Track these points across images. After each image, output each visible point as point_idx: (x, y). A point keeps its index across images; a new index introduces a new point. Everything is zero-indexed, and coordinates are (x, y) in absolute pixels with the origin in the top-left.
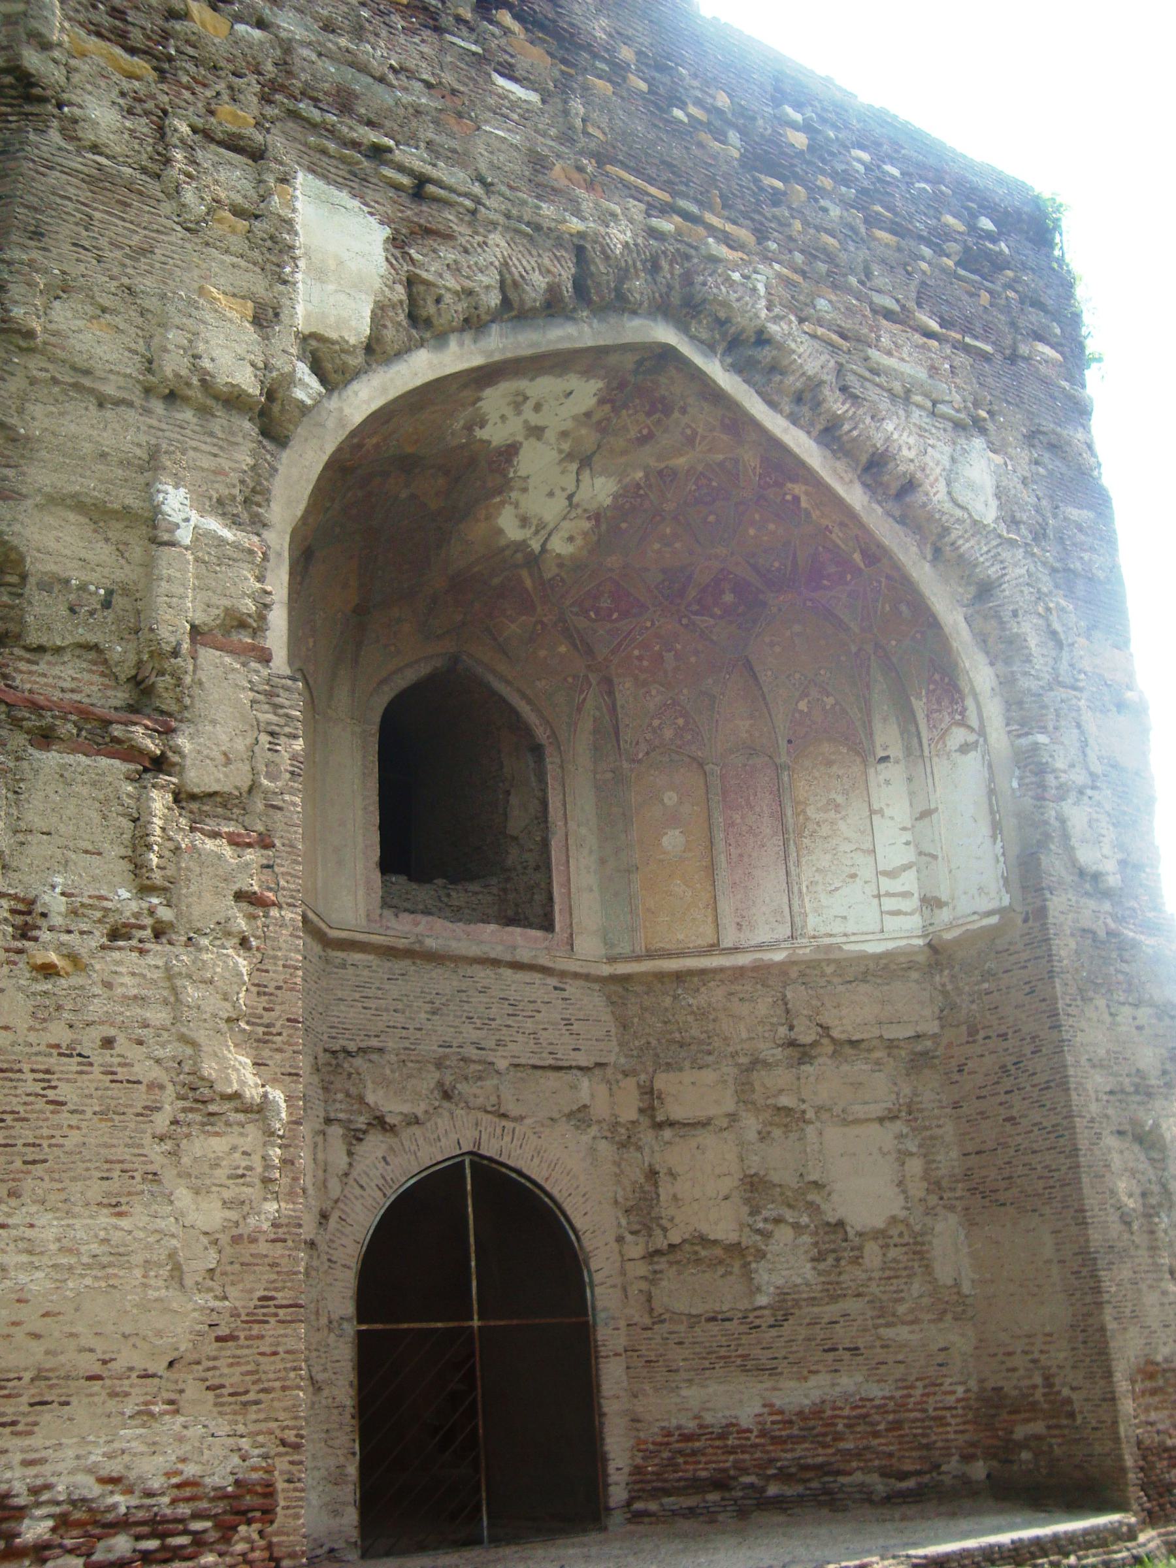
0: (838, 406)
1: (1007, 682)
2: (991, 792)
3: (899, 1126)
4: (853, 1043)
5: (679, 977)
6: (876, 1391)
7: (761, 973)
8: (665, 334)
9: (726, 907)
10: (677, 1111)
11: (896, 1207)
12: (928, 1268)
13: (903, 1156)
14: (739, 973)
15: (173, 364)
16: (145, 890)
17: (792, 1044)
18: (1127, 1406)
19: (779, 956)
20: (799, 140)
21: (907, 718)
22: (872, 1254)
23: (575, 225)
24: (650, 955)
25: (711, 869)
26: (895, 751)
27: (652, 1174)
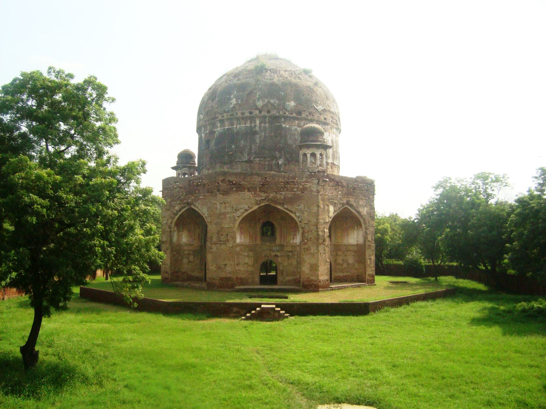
0: (356, 208)
1: (365, 226)
2: (363, 235)
6: (351, 274)
7: (344, 245)
8: (346, 206)
9: (343, 240)
11: (353, 262)
15: (325, 222)
16: (324, 251)
20: (356, 186)
22: (351, 265)
24: (337, 243)
25: (342, 237)
27: (336, 259)
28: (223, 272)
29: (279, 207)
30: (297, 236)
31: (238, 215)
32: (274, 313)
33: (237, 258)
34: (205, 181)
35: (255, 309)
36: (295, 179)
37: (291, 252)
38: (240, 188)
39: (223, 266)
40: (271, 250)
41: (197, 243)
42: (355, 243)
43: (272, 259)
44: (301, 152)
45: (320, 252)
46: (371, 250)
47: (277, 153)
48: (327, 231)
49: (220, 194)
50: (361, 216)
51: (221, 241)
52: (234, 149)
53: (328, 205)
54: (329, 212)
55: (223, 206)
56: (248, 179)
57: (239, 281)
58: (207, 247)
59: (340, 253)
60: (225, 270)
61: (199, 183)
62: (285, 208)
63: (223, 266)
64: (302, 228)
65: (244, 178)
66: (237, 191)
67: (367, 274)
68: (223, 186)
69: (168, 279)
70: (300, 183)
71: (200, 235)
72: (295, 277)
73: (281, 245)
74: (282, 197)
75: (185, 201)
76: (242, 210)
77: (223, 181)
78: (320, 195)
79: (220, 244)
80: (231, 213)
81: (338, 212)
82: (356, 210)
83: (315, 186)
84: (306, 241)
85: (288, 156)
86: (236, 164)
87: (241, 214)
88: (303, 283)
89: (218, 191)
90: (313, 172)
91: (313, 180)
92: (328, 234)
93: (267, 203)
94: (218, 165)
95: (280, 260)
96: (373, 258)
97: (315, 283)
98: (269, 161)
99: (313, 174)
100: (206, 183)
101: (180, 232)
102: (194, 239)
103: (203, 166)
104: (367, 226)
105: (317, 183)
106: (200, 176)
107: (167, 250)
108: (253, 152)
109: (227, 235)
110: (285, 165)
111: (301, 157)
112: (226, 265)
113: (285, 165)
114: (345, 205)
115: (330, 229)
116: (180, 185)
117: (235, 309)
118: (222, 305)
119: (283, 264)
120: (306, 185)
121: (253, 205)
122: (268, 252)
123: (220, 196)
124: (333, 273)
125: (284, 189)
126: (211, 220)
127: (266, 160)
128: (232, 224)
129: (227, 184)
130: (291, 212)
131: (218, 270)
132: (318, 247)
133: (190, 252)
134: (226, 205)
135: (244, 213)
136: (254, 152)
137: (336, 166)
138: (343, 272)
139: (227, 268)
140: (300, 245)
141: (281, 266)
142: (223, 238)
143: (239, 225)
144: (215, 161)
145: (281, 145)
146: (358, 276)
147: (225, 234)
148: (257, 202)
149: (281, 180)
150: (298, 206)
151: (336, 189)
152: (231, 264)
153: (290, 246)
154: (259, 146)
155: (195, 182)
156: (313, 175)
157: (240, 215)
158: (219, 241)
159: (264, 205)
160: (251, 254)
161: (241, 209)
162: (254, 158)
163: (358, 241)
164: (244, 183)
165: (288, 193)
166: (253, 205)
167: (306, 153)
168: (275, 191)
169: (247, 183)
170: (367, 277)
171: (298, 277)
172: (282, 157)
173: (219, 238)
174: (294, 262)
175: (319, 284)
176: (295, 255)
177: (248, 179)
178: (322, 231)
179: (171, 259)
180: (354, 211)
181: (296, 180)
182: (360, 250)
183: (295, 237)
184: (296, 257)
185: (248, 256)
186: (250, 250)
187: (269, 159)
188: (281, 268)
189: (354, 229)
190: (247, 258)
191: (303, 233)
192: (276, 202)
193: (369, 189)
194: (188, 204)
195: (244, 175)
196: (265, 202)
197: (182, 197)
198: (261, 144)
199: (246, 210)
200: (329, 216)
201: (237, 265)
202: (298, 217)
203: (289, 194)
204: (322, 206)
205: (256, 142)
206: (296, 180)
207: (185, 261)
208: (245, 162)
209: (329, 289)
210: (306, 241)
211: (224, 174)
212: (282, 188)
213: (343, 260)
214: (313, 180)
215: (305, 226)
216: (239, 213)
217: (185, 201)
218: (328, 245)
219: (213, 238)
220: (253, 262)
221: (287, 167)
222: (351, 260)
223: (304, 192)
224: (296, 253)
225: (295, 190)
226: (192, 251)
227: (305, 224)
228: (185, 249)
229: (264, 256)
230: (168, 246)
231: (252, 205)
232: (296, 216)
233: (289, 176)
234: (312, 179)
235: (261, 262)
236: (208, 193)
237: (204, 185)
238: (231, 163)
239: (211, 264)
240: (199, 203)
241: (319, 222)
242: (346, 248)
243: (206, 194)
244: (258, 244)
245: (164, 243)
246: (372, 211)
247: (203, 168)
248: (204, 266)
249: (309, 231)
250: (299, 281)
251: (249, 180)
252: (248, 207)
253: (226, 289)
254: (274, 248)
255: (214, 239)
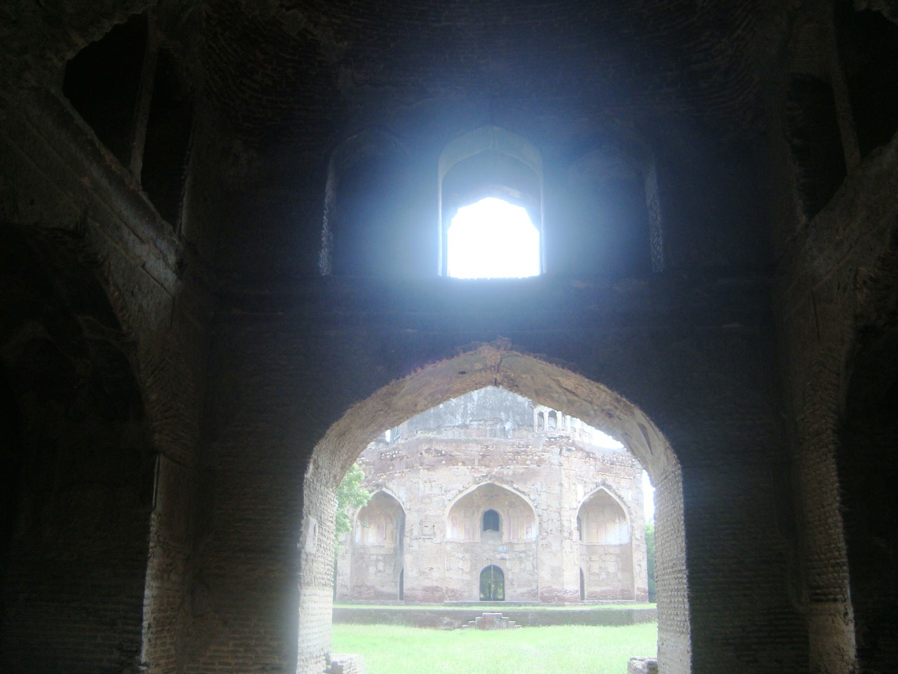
0: (616, 491)
1: (631, 518)
2: (628, 530)
3: (615, 562)
4: (611, 554)
5: (594, 545)
6: (611, 589)
8: (602, 487)
10: (593, 560)
12: (617, 577)
13: (615, 565)
14: (599, 545)
15: (572, 507)
17: (605, 553)
18: (635, 591)
19: (604, 544)
20: (615, 459)
21: (620, 519)
22: (612, 575)
23: (596, 481)
26: (618, 522)
27: (590, 566)
28: (427, 578)
29: (506, 487)
30: (532, 529)
31: (449, 499)
32: (500, 622)
33: (447, 560)
34: (403, 453)
35: (474, 620)
36: (528, 448)
37: (524, 552)
38: (451, 460)
39: (427, 571)
40: (495, 551)
41: (389, 545)
42: (617, 543)
43: (498, 565)
44: (535, 410)
45: (565, 550)
46: (641, 553)
47: (502, 413)
48: (574, 520)
49: (424, 469)
50: (625, 503)
51: (425, 535)
52: (443, 410)
53: (575, 484)
54: (577, 493)
55: (428, 485)
56: (463, 448)
57: (450, 594)
58: (405, 545)
59: (594, 558)
60: (430, 576)
61: (394, 456)
62: (514, 488)
63: (427, 571)
64: (539, 516)
65: (458, 447)
66: (447, 465)
67: (635, 587)
68: (429, 458)
69: (347, 595)
70: (534, 453)
71: (394, 533)
72: (530, 589)
73: (510, 543)
74: (511, 473)
75: (373, 482)
76: (454, 492)
77: (428, 451)
78: (564, 469)
79: (424, 539)
80: (439, 495)
81: (589, 494)
82: (616, 494)
83: (556, 457)
84: (544, 534)
85: (518, 418)
86: (446, 430)
87: (453, 497)
88: (541, 593)
89: (422, 464)
90: (553, 438)
91: (553, 448)
92: (576, 525)
93: (489, 482)
94: (419, 432)
95: (508, 564)
96: (644, 564)
97: (559, 594)
98: (491, 425)
99: (553, 440)
100: (404, 454)
101: (365, 528)
102: (385, 539)
103: (398, 436)
104: (632, 518)
105: (559, 452)
106: (395, 446)
107: (346, 553)
108: (469, 412)
109: (434, 526)
110: (514, 430)
111: (536, 417)
112: (432, 569)
113: (514, 430)
114: (599, 486)
115: (579, 519)
116: (367, 460)
117: (447, 619)
118: (428, 614)
119: (513, 571)
120: (543, 455)
121: (470, 485)
122: (491, 554)
123: (423, 473)
124: (585, 586)
125: (512, 462)
126: (410, 506)
127: (487, 423)
128: (440, 511)
129: (433, 455)
130: (523, 493)
131: (421, 575)
132: (562, 543)
133: (380, 558)
134: (431, 484)
135: (457, 495)
136: (471, 412)
137: (587, 434)
138: (601, 586)
139: (433, 573)
140: (536, 542)
141: (510, 573)
142: (427, 531)
143: (449, 515)
144: (416, 428)
145: (508, 403)
146: (622, 591)
147: (430, 525)
148: (476, 480)
149: (509, 449)
150: (532, 485)
151: (586, 462)
152: (439, 568)
153: (522, 544)
154: (477, 405)
155: (388, 455)
156: (553, 442)
157: (451, 498)
158: (423, 535)
159: (485, 485)
160: (467, 556)
161: (453, 489)
162: (471, 421)
163: (620, 540)
164: (458, 453)
165: (518, 466)
166: (470, 485)
167: (543, 411)
168: (500, 464)
169: (460, 454)
170: (636, 592)
171: (534, 587)
172: (510, 420)
173: (422, 530)
174: (529, 567)
175: (565, 596)
176: (529, 556)
177: (463, 448)
178: (567, 520)
179: (351, 567)
180: (613, 495)
181: (528, 449)
182: (625, 554)
183: (529, 529)
184: (531, 558)
185: (463, 559)
186: (466, 551)
187: (492, 422)
188: (510, 577)
189: (614, 522)
190: (462, 561)
191: (540, 523)
192: (503, 481)
193: (634, 465)
194: (378, 486)
195: (457, 442)
196: (487, 479)
197: (370, 477)
198: (480, 402)
199: (460, 492)
200: (576, 501)
201: (447, 570)
202: (534, 500)
203: (519, 468)
204: (566, 485)
205: (473, 399)
206: (529, 449)
207: (372, 570)
208: (458, 427)
209: (580, 604)
210: (544, 534)
211: (430, 441)
212: (510, 460)
213: (600, 568)
214: (553, 448)
215: (543, 513)
216: (450, 495)
217: (373, 482)
218: (576, 541)
219: (414, 531)
220: (469, 569)
221: (517, 433)
222: (612, 568)
223: (541, 465)
224: (531, 554)
225: (528, 462)
226: (382, 555)
227: (543, 510)
228: (371, 553)
229: (485, 559)
230: (347, 548)
231: (469, 484)
232: (530, 499)
233: (519, 444)
234: (552, 446)
235: (481, 567)
236: (406, 469)
237: (401, 458)
238: (438, 428)
239: (410, 568)
240: (393, 484)
241: (563, 507)
242: (605, 550)
243: (404, 470)
244: (477, 543)
245: (342, 544)
246: (639, 496)
247: (399, 437)
248: (399, 578)
249: (549, 519)
250: (537, 593)
251: (464, 449)
252: (463, 487)
253: (431, 603)
254: (500, 548)
255: (415, 533)
